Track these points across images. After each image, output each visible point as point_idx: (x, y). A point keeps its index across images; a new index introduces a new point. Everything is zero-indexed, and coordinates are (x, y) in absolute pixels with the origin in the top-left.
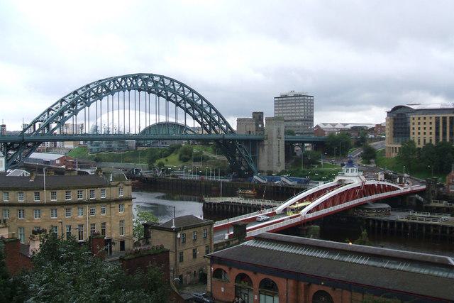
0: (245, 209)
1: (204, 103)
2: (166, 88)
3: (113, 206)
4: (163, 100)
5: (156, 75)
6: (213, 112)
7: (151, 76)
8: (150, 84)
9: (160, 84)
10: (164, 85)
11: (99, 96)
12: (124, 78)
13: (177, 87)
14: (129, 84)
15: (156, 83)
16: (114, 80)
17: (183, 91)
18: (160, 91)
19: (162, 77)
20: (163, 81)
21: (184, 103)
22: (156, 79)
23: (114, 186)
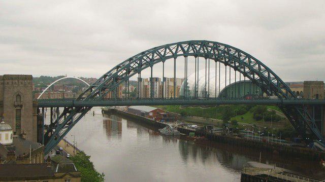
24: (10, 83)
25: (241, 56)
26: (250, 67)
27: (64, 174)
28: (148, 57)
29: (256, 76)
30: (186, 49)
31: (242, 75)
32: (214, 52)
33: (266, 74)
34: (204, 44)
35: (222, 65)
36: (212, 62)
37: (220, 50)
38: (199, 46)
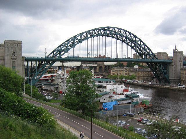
1: (137, 39)
2: (116, 33)
4: (115, 40)
5: (111, 27)
7: (108, 27)
8: (108, 32)
9: (113, 31)
10: (115, 32)
12: (94, 30)
13: (122, 33)
14: (97, 33)
15: (111, 31)
16: (88, 32)
17: (126, 34)
18: (113, 35)
19: (114, 28)
20: (115, 30)
21: (126, 40)
22: (111, 29)
29: (133, 45)
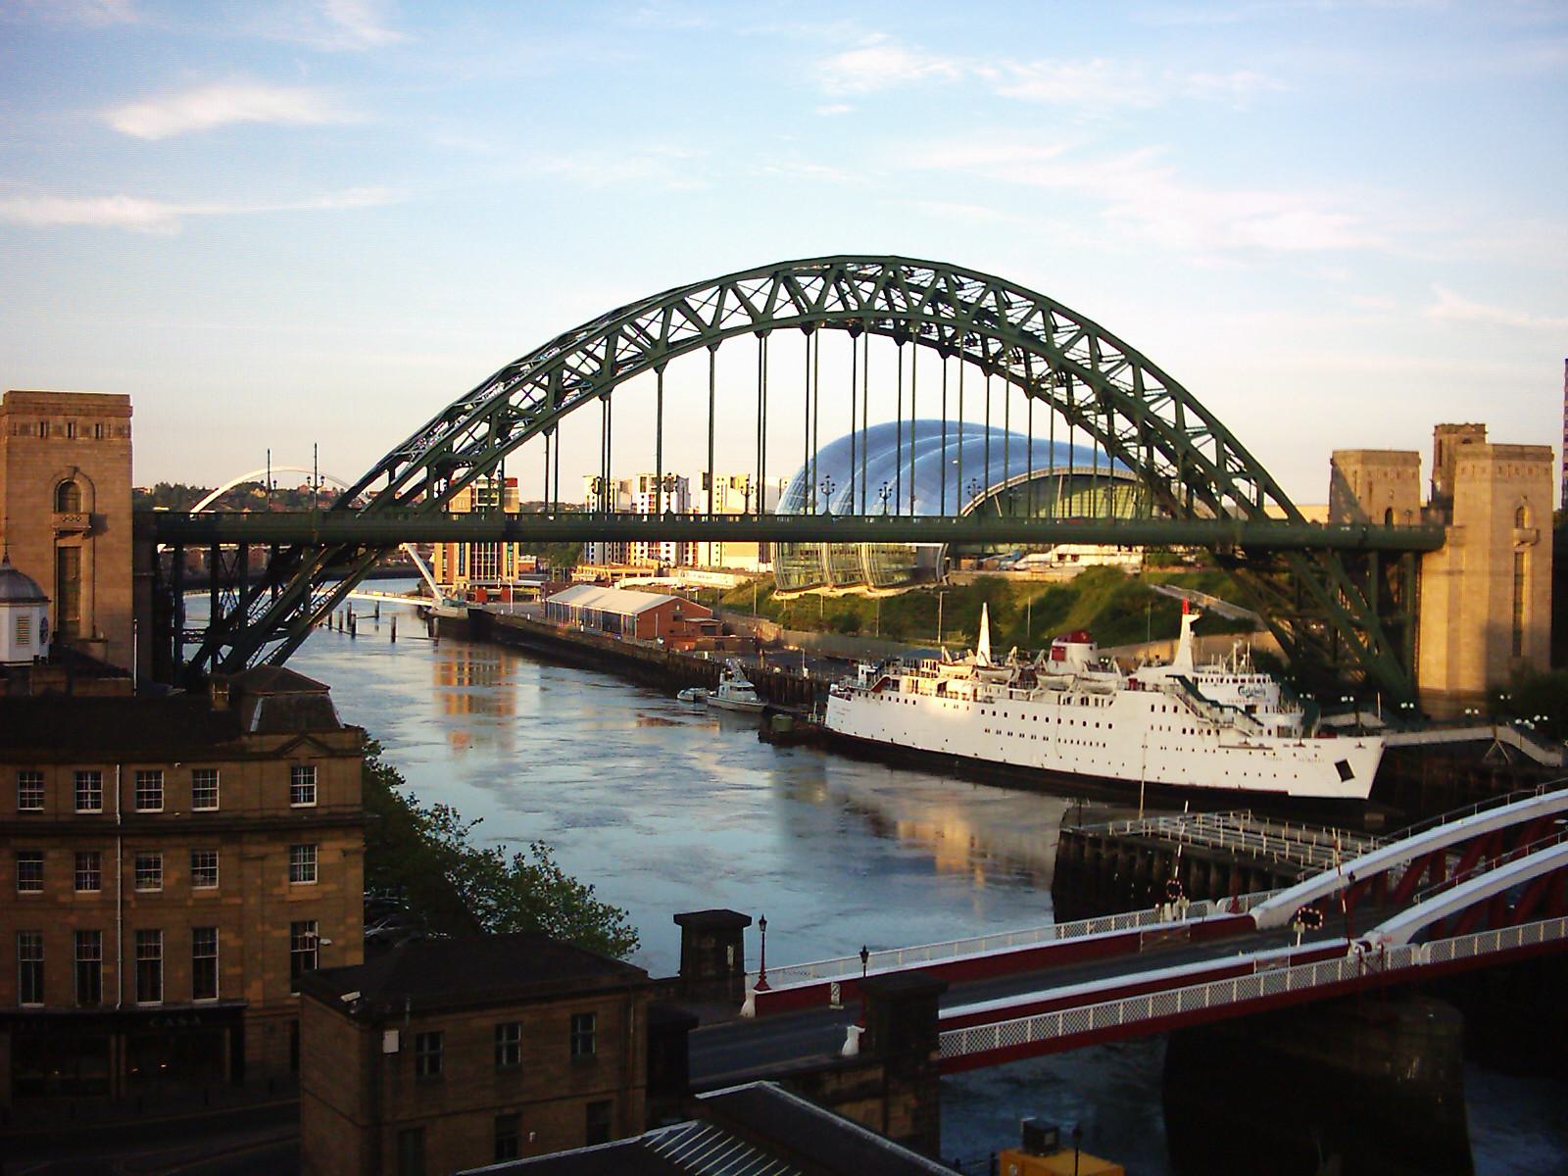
0: (1234, 880)
1: (1150, 382)
3: (254, 850)
6: (1192, 420)
11: (658, 355)
13: (1015, 316)
23: (262, 757)
24: (36, 430)
25: (1009, 305)
26: (1090, 378)
27: (285, 738)
28: (642, 331)
29: (1121, 423)
30: (813, 295)
31: (1059, 417)
32: (937, 312)
33: (1166, 411)
34: (893, 271)
35: (973, 371)
36: (929, 356)
37: (918, 289)
38: (869, 287)
